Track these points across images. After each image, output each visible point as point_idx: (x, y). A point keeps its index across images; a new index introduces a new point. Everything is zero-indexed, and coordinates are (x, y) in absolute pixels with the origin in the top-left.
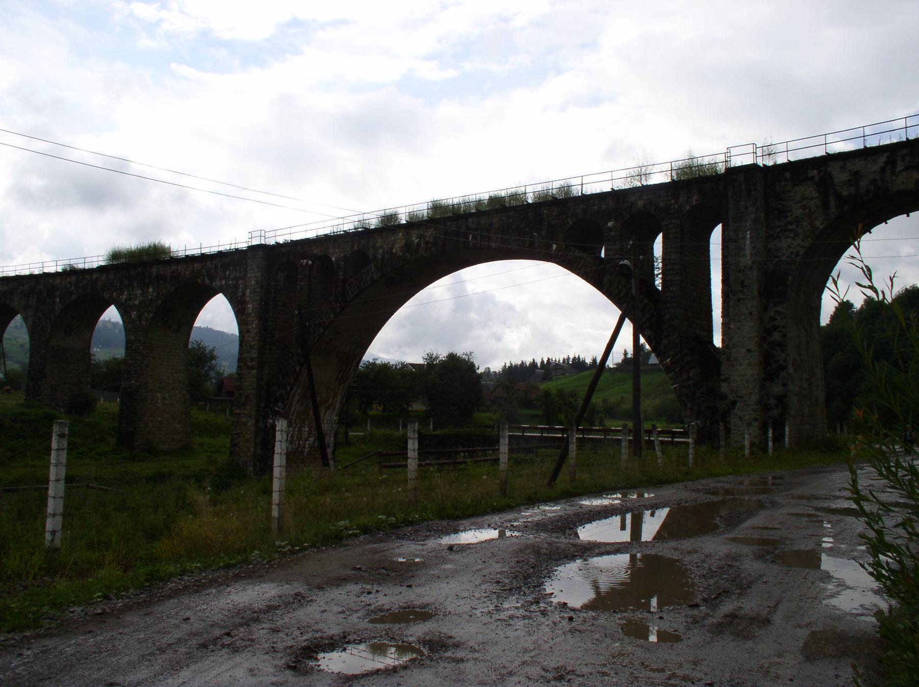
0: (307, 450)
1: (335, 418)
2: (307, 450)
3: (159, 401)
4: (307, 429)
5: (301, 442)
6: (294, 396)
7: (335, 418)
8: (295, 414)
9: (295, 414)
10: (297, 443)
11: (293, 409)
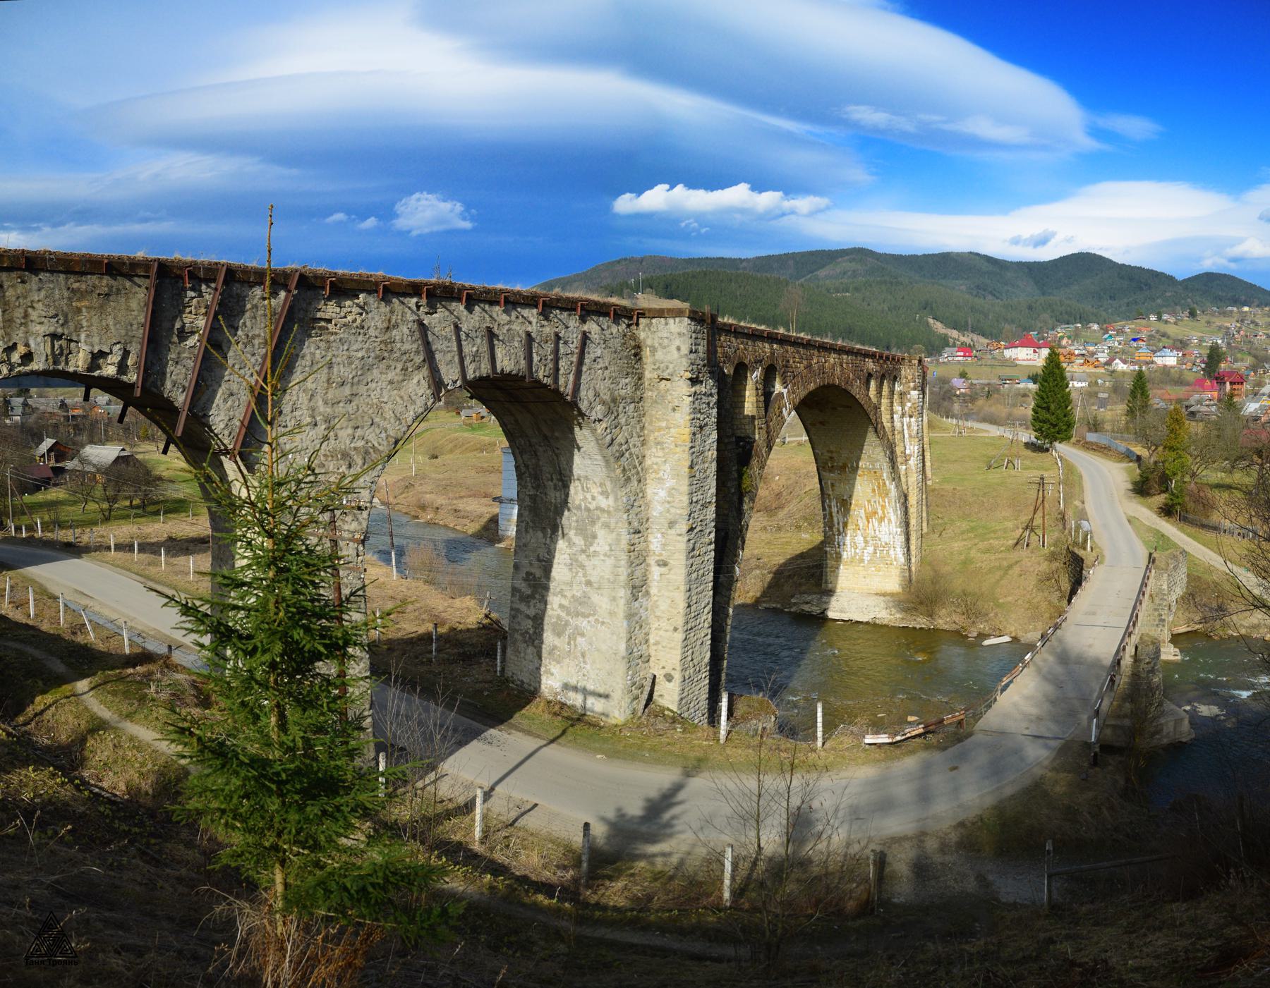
2: (866, 558)
11: (835, 519)
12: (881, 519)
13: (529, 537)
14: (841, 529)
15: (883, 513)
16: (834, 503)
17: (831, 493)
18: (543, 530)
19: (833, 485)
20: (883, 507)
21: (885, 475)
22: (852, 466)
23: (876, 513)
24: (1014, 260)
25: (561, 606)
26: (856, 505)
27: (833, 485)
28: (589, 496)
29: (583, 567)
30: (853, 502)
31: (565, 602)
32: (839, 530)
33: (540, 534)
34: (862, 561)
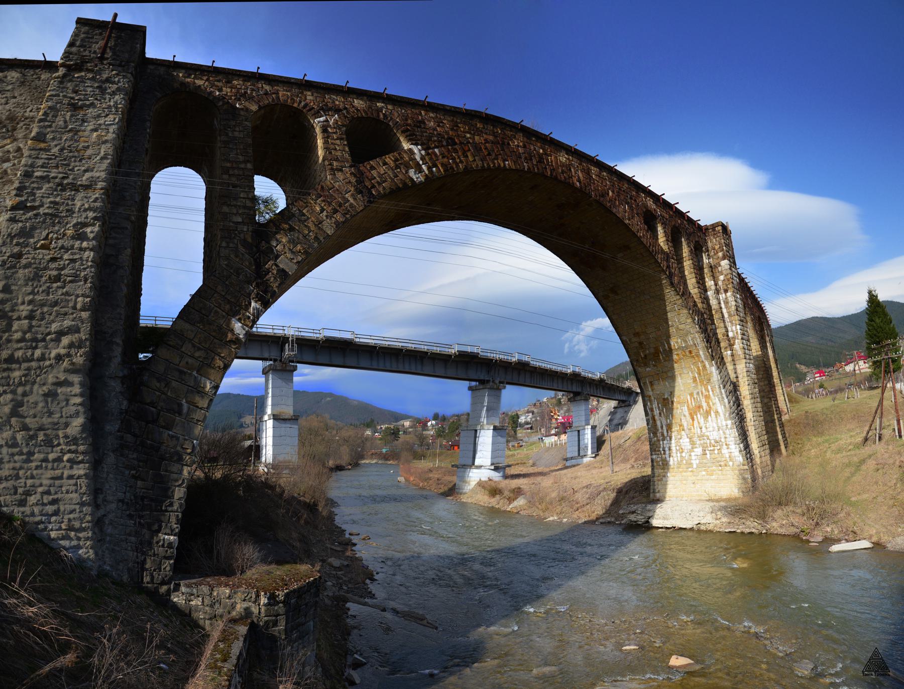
1: (724, 423)
2: (695, 462)
4: (688, 440)
5: (684, 454)
7: (724, 423)
8: (664, 428)
9: (664, 428)
11: (658, 423)
12: (708, 413)
14: (665, 433)
16: (655, 405)
17: (651, 393)
20: (707, 397)
26: (679, 403)
32: (663, 435)
34: (689, 464)
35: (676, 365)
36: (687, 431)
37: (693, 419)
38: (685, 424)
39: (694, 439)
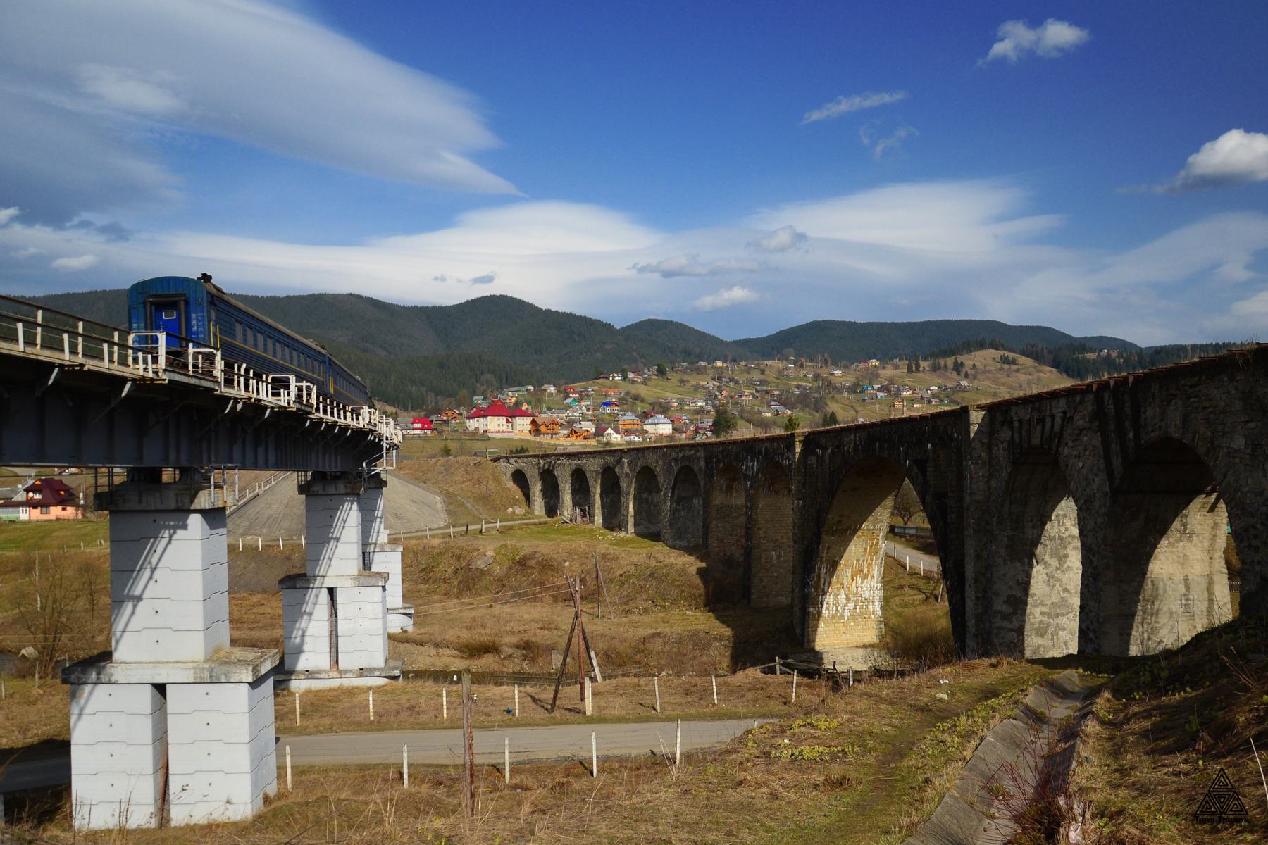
0: (847, 615)
2: (847, 615)
3: (774, 558)
4: (845, 596)
5: (839, 608)
6: (820, 569)
10: (835, 608)
11: (822, 581)
12: (866, 576)
13: (1007, 568)
15: (869, 571)
18: (1021, 561)
19: (829, 548)
20: (870, 565)
21: (881, 535)
22: (855, 528)
23: (861, 571)
24: (407, 304)
25: (1042, 613)
27: (829, 548)
28: (1062, 529)
29: (1059, 580)
30: (842, 562)
31: (1045, 609)
32: (823, 590)
33: (1018, 564)
34: (842, 616)
35: (855, 538)
36: (846, 589)
37: (853, 580)
38: (845, 584)
39: (850, 596)
